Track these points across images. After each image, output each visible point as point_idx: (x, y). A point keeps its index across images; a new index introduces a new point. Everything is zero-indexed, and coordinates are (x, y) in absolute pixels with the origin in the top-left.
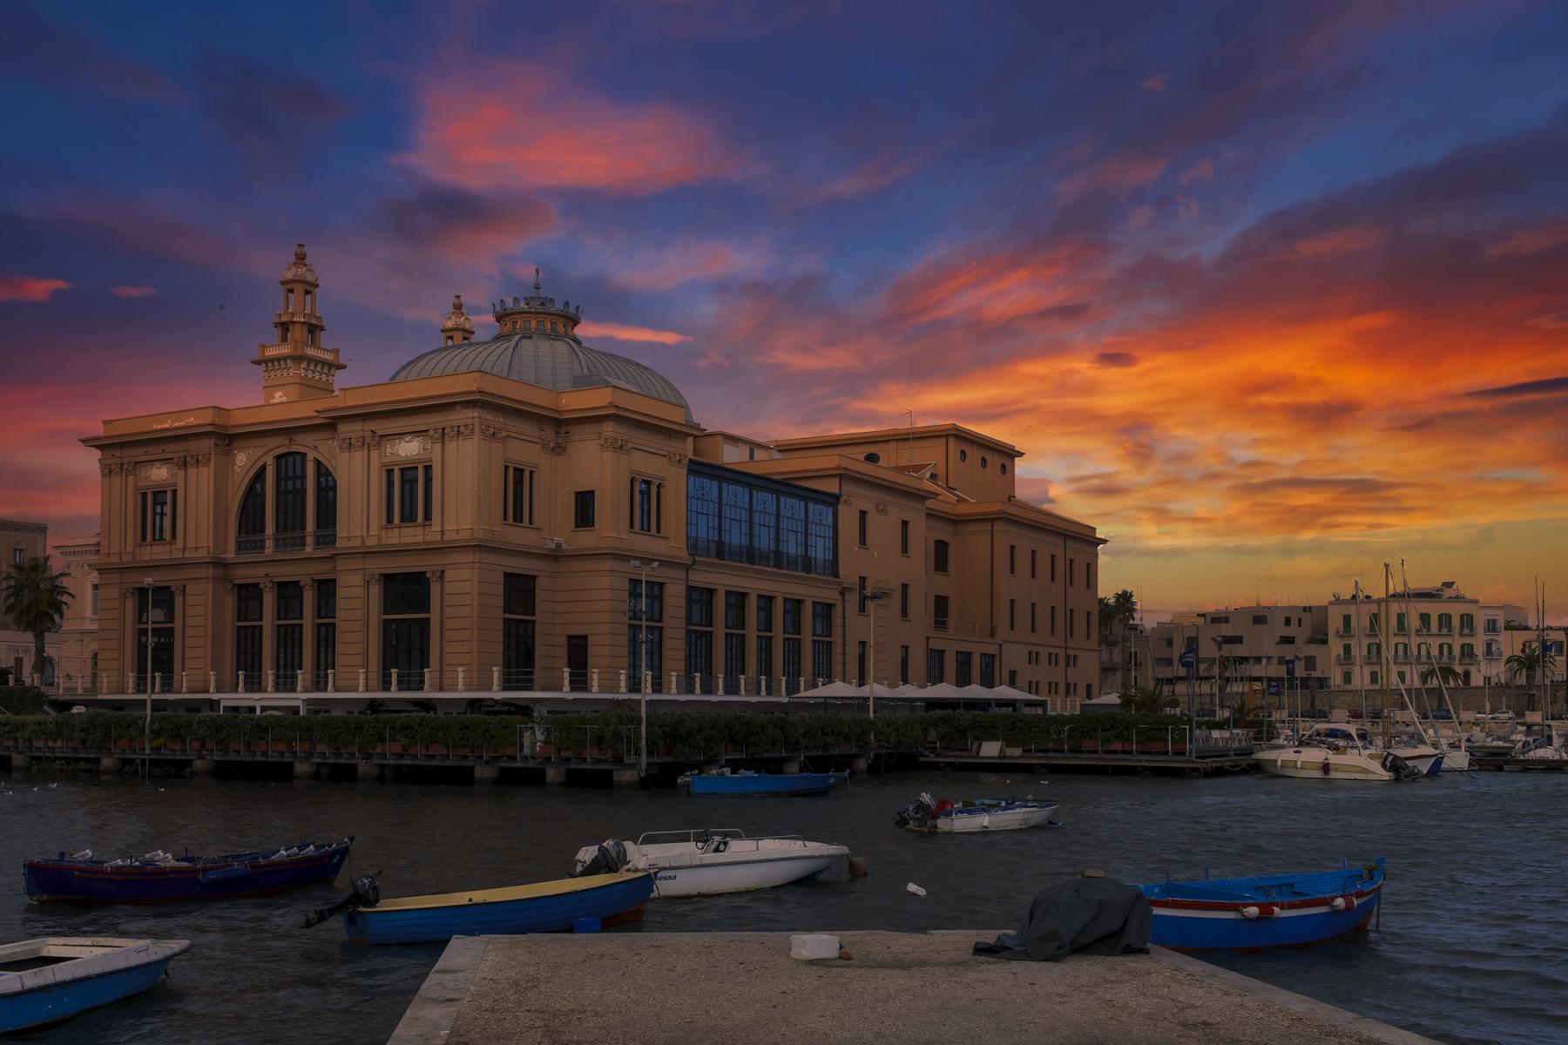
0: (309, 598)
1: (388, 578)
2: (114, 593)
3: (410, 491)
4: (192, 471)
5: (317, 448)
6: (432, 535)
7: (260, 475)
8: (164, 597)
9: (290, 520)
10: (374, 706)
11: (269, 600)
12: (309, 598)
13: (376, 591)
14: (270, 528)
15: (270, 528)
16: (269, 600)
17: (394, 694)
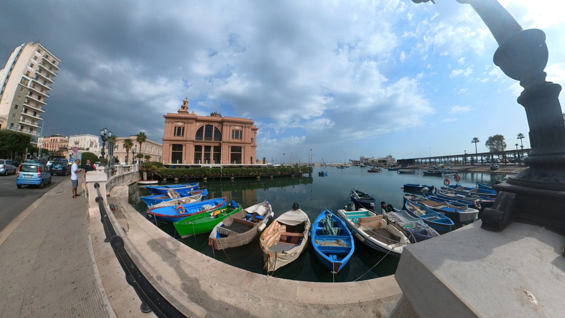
0: (212, 149)
1: (232, 147)
2: (168, 145)
3: (237, 134)
4: (190, 125)
5: (215, 125)
6: (243, 141)
7: (202, 127)
8: (180, 147)
9: (208, 135)
10: (231, 167)
11: (203, 149)
12: (212, 149)
13: (230, 149)
14: (204, 136)
15: (204, 136)
16: (203, 149)
17: (235, 164)
